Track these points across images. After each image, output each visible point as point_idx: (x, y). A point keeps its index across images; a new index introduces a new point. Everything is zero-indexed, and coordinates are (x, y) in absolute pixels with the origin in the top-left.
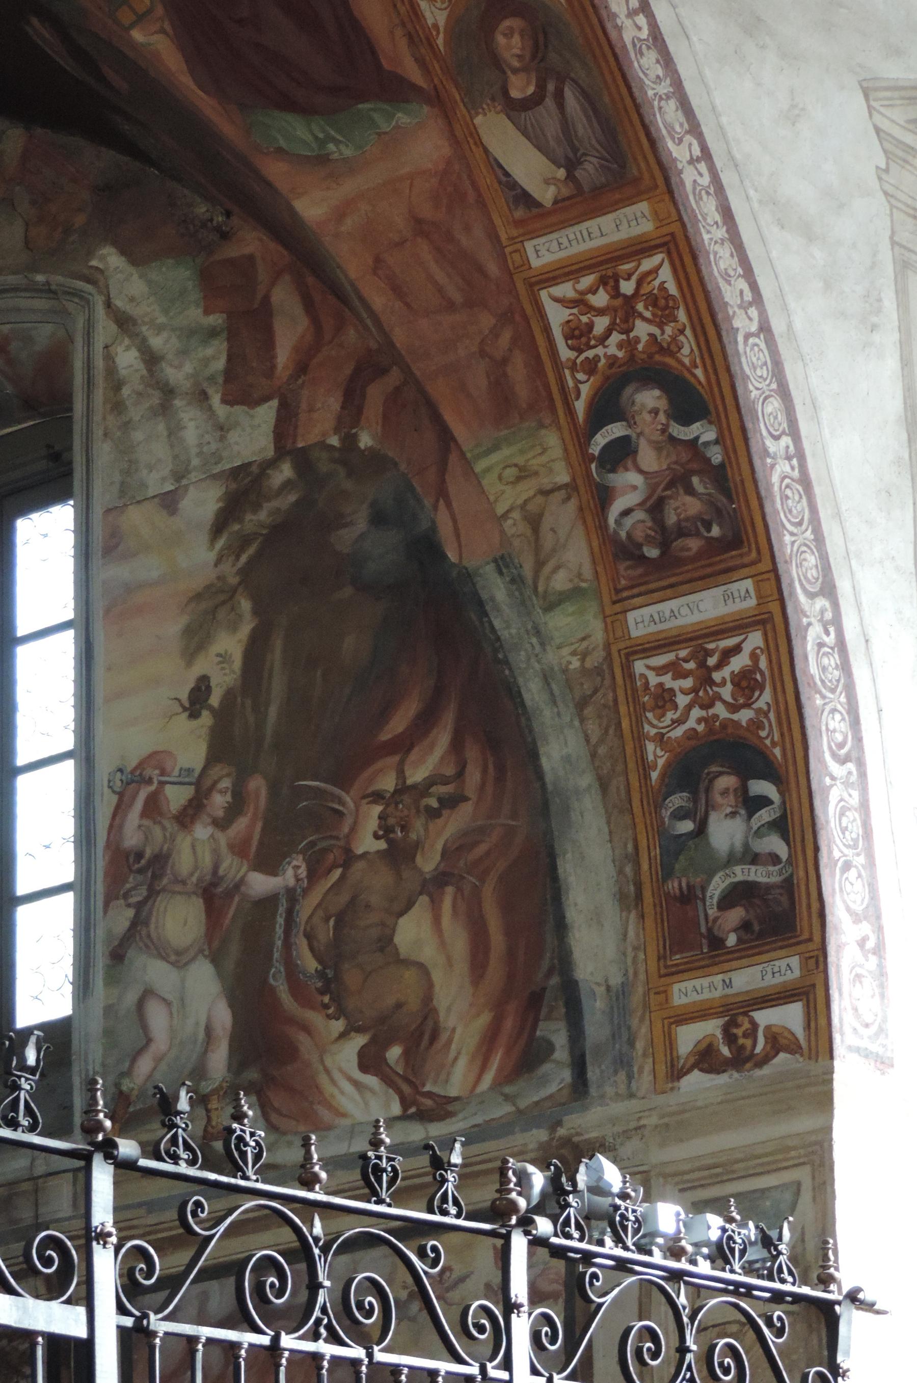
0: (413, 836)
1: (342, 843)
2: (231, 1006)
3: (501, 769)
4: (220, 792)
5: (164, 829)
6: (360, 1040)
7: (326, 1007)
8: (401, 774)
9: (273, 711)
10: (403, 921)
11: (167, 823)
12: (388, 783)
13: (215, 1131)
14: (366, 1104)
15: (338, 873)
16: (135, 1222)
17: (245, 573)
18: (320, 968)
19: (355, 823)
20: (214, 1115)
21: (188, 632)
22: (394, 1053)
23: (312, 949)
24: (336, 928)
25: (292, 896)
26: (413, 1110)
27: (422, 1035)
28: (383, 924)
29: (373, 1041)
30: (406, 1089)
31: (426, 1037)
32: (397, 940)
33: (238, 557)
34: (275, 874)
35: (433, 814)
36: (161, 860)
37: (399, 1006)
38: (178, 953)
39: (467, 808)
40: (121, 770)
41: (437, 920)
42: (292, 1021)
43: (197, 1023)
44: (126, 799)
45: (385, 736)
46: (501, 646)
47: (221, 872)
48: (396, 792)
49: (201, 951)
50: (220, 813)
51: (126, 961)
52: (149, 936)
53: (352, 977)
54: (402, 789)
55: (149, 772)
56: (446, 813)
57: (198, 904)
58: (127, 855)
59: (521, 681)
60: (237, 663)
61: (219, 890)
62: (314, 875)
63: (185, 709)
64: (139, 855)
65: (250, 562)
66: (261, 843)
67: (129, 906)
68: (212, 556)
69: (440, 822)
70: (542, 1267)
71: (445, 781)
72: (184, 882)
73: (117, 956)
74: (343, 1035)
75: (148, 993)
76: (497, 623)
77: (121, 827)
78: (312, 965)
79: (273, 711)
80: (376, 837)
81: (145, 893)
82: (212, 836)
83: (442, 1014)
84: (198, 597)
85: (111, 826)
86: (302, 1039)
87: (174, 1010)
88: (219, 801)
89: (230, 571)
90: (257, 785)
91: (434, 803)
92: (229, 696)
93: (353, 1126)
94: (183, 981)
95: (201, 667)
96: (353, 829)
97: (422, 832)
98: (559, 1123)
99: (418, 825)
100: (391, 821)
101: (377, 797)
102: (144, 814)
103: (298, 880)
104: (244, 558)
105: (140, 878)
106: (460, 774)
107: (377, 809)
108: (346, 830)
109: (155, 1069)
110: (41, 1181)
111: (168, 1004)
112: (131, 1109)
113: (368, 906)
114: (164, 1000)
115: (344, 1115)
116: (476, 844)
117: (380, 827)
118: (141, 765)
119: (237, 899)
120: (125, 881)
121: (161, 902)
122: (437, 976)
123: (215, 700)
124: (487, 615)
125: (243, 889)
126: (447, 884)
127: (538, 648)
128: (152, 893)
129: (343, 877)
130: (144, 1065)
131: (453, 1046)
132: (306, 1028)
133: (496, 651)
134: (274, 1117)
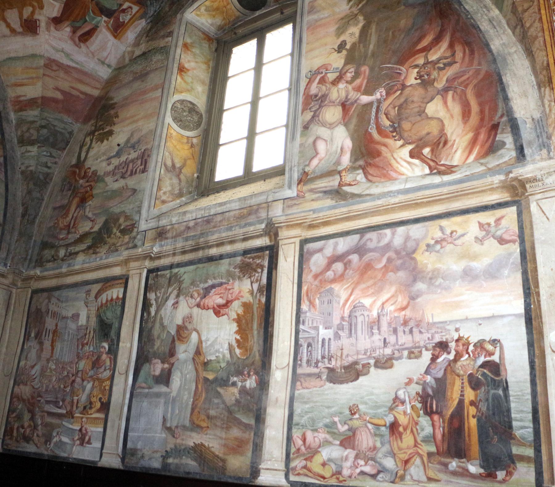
0: (433, 77)
1: (401, 83)
2: (352, 139)
3: (472, 52)
4: (350, 73)
5: (326, 86)
6: (410, 147)
7: (395, 137)
8: (426, 57)
9: (371, 47)
10: (429, 105)
11: (328, 85)
12: (421, 61)
13: (343, 183)
14: (413, 170)
15: (399, 92)
16: (307, 217)
17: (361, 10)
18: (391, 124)
19: (406, 76)
20: (343, 178)
21: (338, 29)
22: (426, 151)
23: (388, 118)
24: (398, 110)
25: (379, 102)
26: (435, 171)
27: (439, 144)
28: (420, 106)
29: (417, 146)
30: (432, 164)
31: (441, 145)
32: (426, 111)
33: (358, 6)
34: (372, 95)
35: (441, 69)
36: (324, 97)
37: (428, 134)
38: (330, 124)
39: (458, 65)
40: (311, 72)
41: (445, 103)
42: (378, 143)
43: (337, 147)
44: (312, 80)
45: (420, 47)
46: (469, 14)
47: (349, 97)
48: (424, 64)
49: (340, 123)
50: (350, 79)
51: (309, 129)
52: (319, 120)
53: (406, 125)
54: (427, 63)
55: (321, 71)
56: (447, 68)
57: (340, 108)
58: (311, 96)
59: (479, 23)
60: (357, 35)
61: (348, 103)
62: (388, 94)
63: (336, 51)
64: (316, 96)
65: (363, 6)
66: (366, 86)
67: (311, 111)
68: (348, 7)
69: (444, 71)
70: (505, 230)
71: (446, 58)
72: (334, 102)
73: (306, 127)
74: (402, 146)
75: (318, 138)
76: (467, 7)
77: (309, 88)
78: (388, 123)
79: (371, 47)
80: (416, 79)
81: (318, 107)
82: (346, 86)
83: (449, 136)
84: (342, 19)
85: (306, 89)
86: (383, 149)
87: (328, 143)
88: (349, 76)
89: (355, 10)
90: (365, 69)
91: (442, 66)
92: (354, 45)
93: (407, 178)
94: (332, 133)
95: (342, 38)
96: (405, 78)
97: (437, 75)
98: (511, 172)
99: (435, 74)
100: (422, 73)
101: (416, 66)
102: (319, 83)
103: (381, 96)
104: (360, 6)
105: (316, 102)
106: (453, 55)
107: (416, 70)
108: (403, 78)
109: (318, 164)
110: (270, 203)
111: (326, 141)
112: (309, 177)
113: (413, 101)
114: (324, 140)
115: (403, 175)
116: (462, 76)
117: (417, 76)
118: (318, 69)
119: (356, 105)
120: (311, 104)
121: (324, 109)
122: (446, 122)
123: (348, 47)
124: (462, 5)
125: (358, 101)
126: (449, 90)
127: (486, 12)
128: (320, 107)
129: (401, 94)
130: (315, 162)
131: (455, 146)
132: (385, 145)
133: (467, 15)
134: (370, 177)
